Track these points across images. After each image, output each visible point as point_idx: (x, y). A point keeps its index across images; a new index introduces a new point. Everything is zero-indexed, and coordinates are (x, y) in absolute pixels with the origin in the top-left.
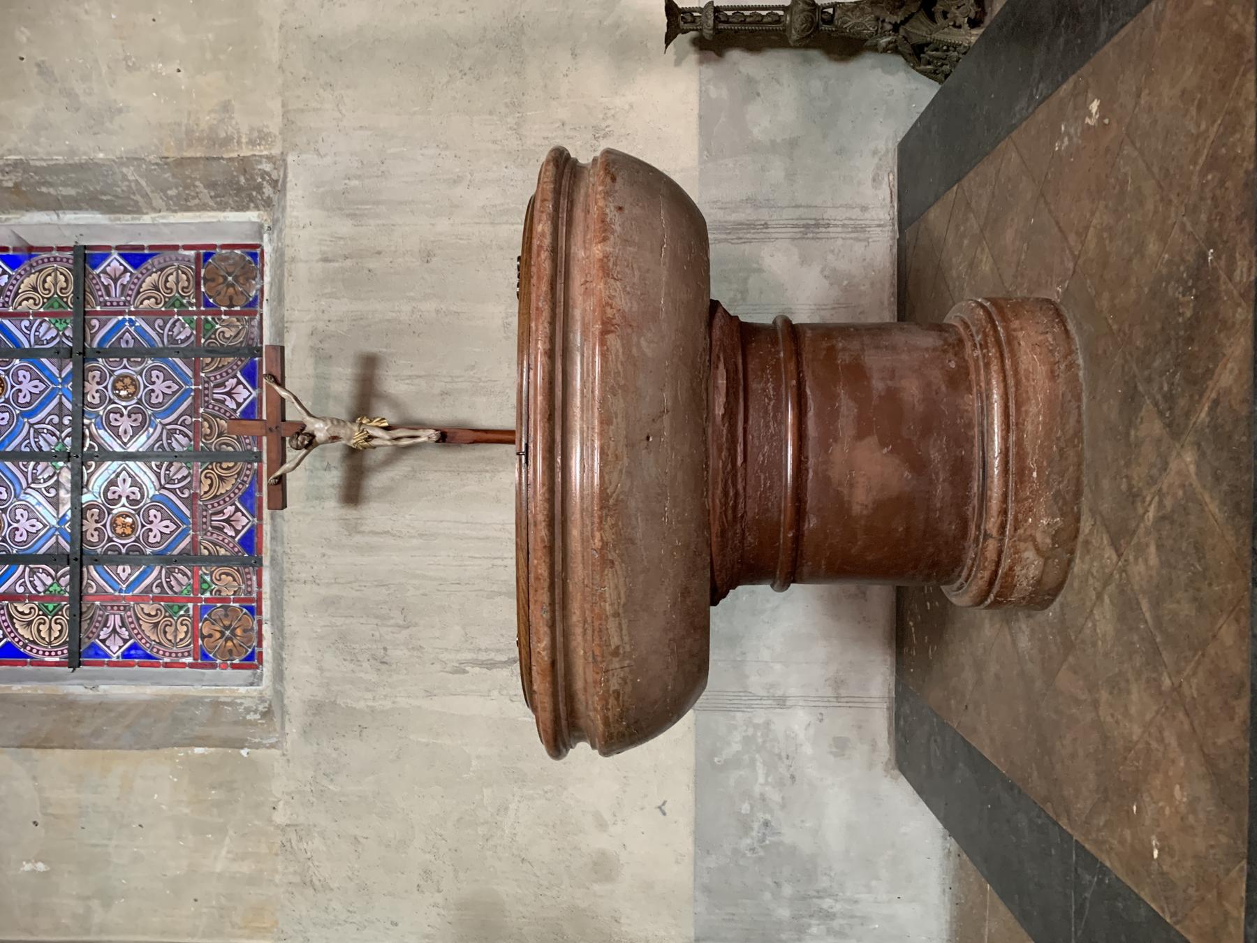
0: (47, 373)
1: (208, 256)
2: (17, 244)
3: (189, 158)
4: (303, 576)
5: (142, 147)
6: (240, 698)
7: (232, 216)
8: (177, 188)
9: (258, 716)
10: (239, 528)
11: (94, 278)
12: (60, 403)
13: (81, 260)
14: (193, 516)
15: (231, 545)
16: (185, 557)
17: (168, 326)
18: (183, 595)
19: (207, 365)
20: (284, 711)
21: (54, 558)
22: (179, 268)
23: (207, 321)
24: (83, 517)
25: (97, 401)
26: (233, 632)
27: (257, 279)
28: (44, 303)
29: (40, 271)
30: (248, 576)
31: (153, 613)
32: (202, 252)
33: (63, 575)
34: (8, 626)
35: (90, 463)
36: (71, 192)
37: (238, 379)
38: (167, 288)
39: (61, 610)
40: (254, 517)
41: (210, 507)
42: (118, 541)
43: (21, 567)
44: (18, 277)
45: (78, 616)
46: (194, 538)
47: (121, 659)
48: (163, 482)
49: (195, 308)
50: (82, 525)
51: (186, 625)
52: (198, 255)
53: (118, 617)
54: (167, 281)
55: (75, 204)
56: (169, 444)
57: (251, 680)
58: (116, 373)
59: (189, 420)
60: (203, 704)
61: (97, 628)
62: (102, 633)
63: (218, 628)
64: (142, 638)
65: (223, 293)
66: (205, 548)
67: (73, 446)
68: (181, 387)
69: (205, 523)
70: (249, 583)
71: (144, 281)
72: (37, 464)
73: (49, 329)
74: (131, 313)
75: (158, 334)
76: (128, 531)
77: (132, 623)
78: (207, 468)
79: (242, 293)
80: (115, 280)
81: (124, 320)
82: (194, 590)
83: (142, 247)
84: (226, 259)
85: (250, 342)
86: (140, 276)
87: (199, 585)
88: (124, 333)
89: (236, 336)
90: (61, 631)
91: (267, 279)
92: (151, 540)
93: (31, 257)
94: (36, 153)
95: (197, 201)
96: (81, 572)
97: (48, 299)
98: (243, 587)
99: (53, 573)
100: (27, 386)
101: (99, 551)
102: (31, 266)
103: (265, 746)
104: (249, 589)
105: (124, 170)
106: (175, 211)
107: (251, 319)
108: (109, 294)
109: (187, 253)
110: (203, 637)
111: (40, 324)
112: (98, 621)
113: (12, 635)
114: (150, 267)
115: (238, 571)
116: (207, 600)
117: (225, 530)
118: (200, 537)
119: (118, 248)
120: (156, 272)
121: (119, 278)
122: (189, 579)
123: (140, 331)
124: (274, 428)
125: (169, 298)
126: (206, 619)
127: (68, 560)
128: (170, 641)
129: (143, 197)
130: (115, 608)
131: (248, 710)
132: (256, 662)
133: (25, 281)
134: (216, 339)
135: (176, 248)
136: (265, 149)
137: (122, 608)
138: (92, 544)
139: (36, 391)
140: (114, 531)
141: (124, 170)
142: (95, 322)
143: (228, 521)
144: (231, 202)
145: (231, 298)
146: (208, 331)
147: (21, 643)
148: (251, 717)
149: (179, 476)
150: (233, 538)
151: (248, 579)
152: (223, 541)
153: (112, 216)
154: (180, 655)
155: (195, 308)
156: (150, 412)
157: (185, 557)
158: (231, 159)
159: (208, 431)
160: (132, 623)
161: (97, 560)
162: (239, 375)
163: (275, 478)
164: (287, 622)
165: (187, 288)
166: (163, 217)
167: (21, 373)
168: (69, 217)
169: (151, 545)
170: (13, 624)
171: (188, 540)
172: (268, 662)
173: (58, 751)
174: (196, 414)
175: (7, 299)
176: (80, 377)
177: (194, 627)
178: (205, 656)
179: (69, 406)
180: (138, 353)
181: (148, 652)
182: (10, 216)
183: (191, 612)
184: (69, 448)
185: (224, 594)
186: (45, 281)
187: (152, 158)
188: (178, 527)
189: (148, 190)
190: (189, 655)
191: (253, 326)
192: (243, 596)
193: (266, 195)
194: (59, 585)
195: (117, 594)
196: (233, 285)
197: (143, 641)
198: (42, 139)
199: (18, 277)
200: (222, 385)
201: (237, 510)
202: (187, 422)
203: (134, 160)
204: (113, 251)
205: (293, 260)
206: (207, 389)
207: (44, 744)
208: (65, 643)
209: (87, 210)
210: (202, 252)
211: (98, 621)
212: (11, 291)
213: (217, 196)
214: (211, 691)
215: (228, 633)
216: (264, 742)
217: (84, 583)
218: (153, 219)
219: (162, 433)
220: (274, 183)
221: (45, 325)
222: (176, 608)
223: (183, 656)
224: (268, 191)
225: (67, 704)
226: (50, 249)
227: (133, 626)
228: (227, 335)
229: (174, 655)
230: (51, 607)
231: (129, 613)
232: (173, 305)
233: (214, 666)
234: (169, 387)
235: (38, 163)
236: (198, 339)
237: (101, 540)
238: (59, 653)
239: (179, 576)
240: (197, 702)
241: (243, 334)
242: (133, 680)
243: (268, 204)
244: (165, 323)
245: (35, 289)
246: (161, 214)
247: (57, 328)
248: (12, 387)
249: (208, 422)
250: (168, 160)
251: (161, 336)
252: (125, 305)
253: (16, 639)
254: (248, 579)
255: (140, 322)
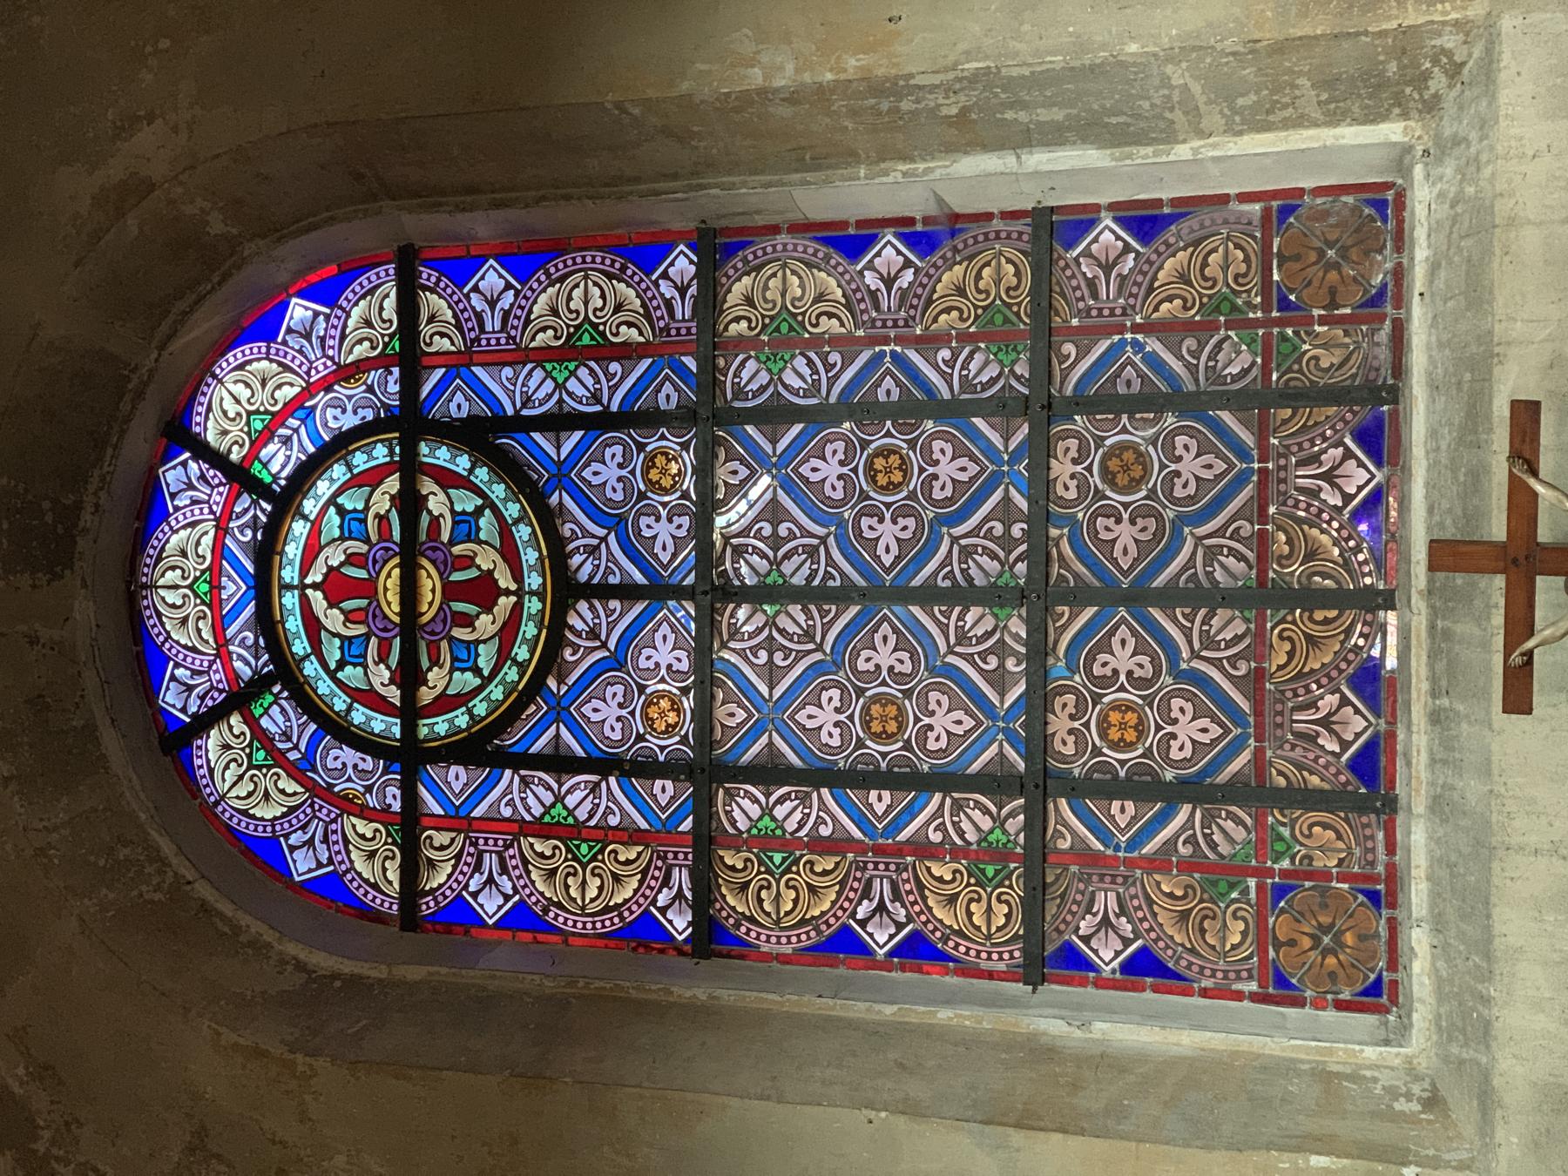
0: (983, 445)
1: (1286, 211)
2: (932, 210)
3: (1300, 38)
4: (1533, 840)
5: (1210, 25)
6: (1370, 1067)
7: (1350, 134)
8: (1257, 93)
9: (1415, 1107)
10: (1349, 737)
11: (1067, 266)
12: (1007, 498)
13: (1045, 236)
14: (1258, 712)
15: (1333, 770)
16: (1235, 792)
17: (1208, 349)
18: (1237, 861)
19: (1285, 422)
20: (1486, 1098)
21: (996, 783)
22: (1228, 238)
23: (1284, 338)
24: (1047, 707)
25: (1072, 494)
26: (1337, 938)
27: (1387, 252)
28: (977, 317)
29: (970, 258)
30: (1368, 832)
31: (1179, 893)
32: (1275, 204)
33: (1012, 815)
34: (916, 902)
35: (1059, 609)
36: (1058, 115)
37: (1347, 448)
38: (1206, 279)
39: (1009, 877)
40: (1378, 715)
41: (1289, 694)
42: (1113, 755)
43: (938, 797)
44: (932, 271)
45: (1040, 889)
46: (1259, 753)
47: (1118, 975)
48: (1197, 645)
49: (1259, 314)
50: (1046, 723)
51: (1244, 919)
52: (1267, 212)
53: (1112, 896)
54: (1205, 264)
55: (1054, 136)
56: (1209, 575)
57: (1382, 1034)
58: (1108, 442)
59: (1247, 529)
60: (1299, 1074)
61: (1074, 914)
62: (1083, 924)
63: (1307, 930)
64: (1159, 939)
65: (1316, 283)
66: (1280, 773)
67: (1029, 577)
68: (1231, 466)
69: (1281, 726)
70: (1370, 844)
71: (1161, 268)
72: (966, 610)
73: (986, 363)
74: (1136, 328)
75: (1188, 365)
76: (1131, 736)
77: (1140, 908)
78: (1283, 621)
79: (1354, 279)
80: (1107, 268)
81: (1123, 342)
82: (1260, 852)
83: (1158, 203)
84: (1324, 215)
85: (1372, 376)
86: (1154, 257)
87: (1264, 841)
88: (1123, 366)
89: (1341, 365)
90: (1008, 916)
91: (1421, 254)
92: (1175, 754)
93: (953, 234)
94: (1017, 54)
95: (1289, 112)
96: (1045, 808)
97: (985, 308)
98: (1357, 852)
99: (994, 809)
100: (948, 469)
101: (1076, 772)
102: (955, 250)
103: (1447, 1165)
104: (1370, 857)
105: (1169, 69)
106: (1240, 133)
107: (1374, 332)
108: (1095, 295)
109: (1246, 207)
110: (1278, 946)
111: (971, 354)
112: (1075, 902)
113: (923, 918)
114: (1172, 240)
115: (1347, 820)
116: (1284, 873)
117: (1320, 741)
118: (1269, 753)
119: (1112, 207)
120: (1185, 249)
121: (1115, 263)
122: (1249, 833)
123: (1154, 361)
124: (1522, 560)
125: (1210, 297)
126: (1283, 911)
127: (1022, 786)
128: (1213, 947)
129: (1186, 113)
130: (1108, 879)
131: (1392, 1092)
132: (1384, 999)
133: (944, 278)
134: (1300, 371)
135: (1224, 199)
136: (1454, 9)
137: (1120, 880)
138: (1064, 759)
139: (963, 477)
140: (1103, 735)
141: (1169, 69)
142: (1069, 348)
143: (1325, 722)
144: (1356, 109)
145: (1333, 292)
146: (1287, 356)
147: (938, 934)
148: (1401, 1105)
149: (1228, 635)
150: (1337, 756)
151: (1366, 838)
152: (1316, 760)
153: (1117, 152)
154: (1232, 975)
155: (1259, 314)
156: (1171, 515)
157: (1235, 792)
158: (1382, 34)
159: (1286, 549)
160: (1140, 908)
161: (1077, 790)
162: (1348, 441)
163: (1523, 654)
164: (1498, 928)
165: (1245, 275)
166: (1214, 146)
167: (937, 445)
168: (1039, 159)
169: (1174, 764)
170: (924, 899)
171: (1245, 757)
172: (1423, 1002)
173: (1057, 1137)
174: (1263, 517)
175: (912, 312)
176: (1040, 451)
177: (1261, 919)
178: (1282, 981)
179: (1023, 504)
180: (1148, 403)
181: (1170, 965)
182: (931, 165)
183: (1253, 895)
184: (1022, 582)
185: (1318, 864)
186: (979, 277)
187: (1230, 44)
188: (1227, 731)
189: (1201, 100)
190: (1250, 977)
191: (1378, 344)
192: (1356, 869)
193: (1432, 91)
194: (1005, 832)
195: (1110, 852)
196: (1336, 266)
197: (1162, 944)
198: (1026, 27)
199: (932, 271)
200: (1315, 459)
201: (1344, 701)
202: (1242, 532)
203: (1189, 50)
204: (1103, 214)
205: (1512, 222)
206: (1285, 468)
207: (1027, 1121)
208: (1016, 937)
209: (1074, 143)
210: (1275, 204)
211: (1075, 902)
212: (919, 297)
213: (1327, 102)
214: (1308, 1050)
215: (1326, 940)
216: (1447, 1157)
217: (1050, 832)
218: (1195, 151)
219: (1194, 553)
220: (1455, 71)
221: (979, 358)
222: (1223, 886)
223: (1239, 978)
224: (1438, 82)
225: (1041, 1052)
226: (988, 216)
227: (1140, 914)
228: (1325, 364)
229: (1219, 975)
230: (990, 871)
231: (1132, 891)
232: (1217, 310)
233: (1299, 1003)
234: (1210, 467)
235: (1015, 72)
236: (1266, 372)
237: (1079, 753)
238: (1006, 956)
239: (1229, 825)
240: (1286, 1068)
241: (1356, 359)
242: (1149, 1017)
243: (1431, 106)
244: (1202, 345)
245: (961, 291)
246: (1211, 140)
247: (1001, 362)
248: (921, 470)
249: (1286, 532)
250: (1258, 45)
251: (1192, 369)
252: (1124, 314)
253: (930, 927)
254: (1366, 838)
255: (1153, 345)
